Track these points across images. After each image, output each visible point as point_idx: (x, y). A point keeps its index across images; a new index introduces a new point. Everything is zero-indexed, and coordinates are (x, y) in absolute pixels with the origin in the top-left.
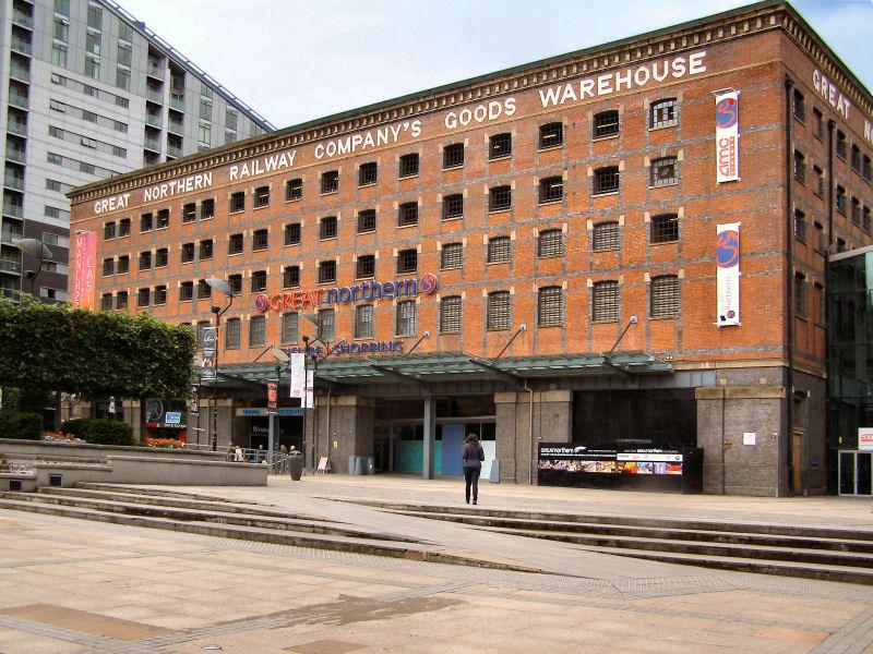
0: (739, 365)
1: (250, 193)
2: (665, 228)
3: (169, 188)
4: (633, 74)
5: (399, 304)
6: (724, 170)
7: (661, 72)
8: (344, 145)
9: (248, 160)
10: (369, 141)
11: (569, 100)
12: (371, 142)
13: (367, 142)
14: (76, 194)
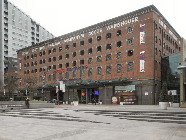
0: (144, 79)
1: (52, 50)
2: (130, 53)
4: (124, 22)
5: (81, 70)
6: (142, 41)
7: (130, 22)
8: (70, 39)
9: (51, 43)
13: (74, 39)
14: (18, 51)
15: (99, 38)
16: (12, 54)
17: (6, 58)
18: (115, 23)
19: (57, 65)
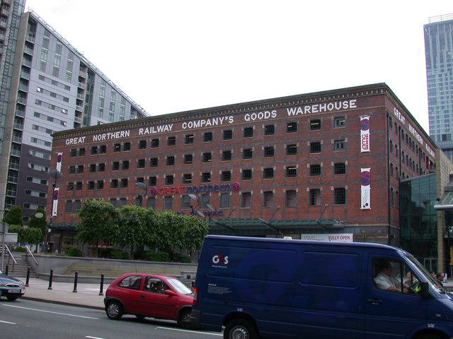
2: (340, 168)
3: (107, 136)
7: (338, 106)
9: (149, 127)
10: (209, 122)
11: (300, 114)
12: (210, 123)
15: (270, 129)
16: (35, 135)
17: (16, 146)
18: (307, 105)
19: (161, 177)
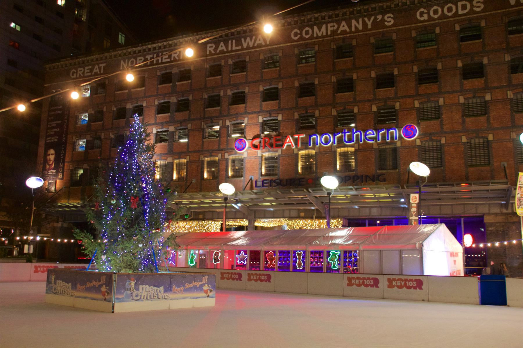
12: (346, 28)
13: (341, 28)
